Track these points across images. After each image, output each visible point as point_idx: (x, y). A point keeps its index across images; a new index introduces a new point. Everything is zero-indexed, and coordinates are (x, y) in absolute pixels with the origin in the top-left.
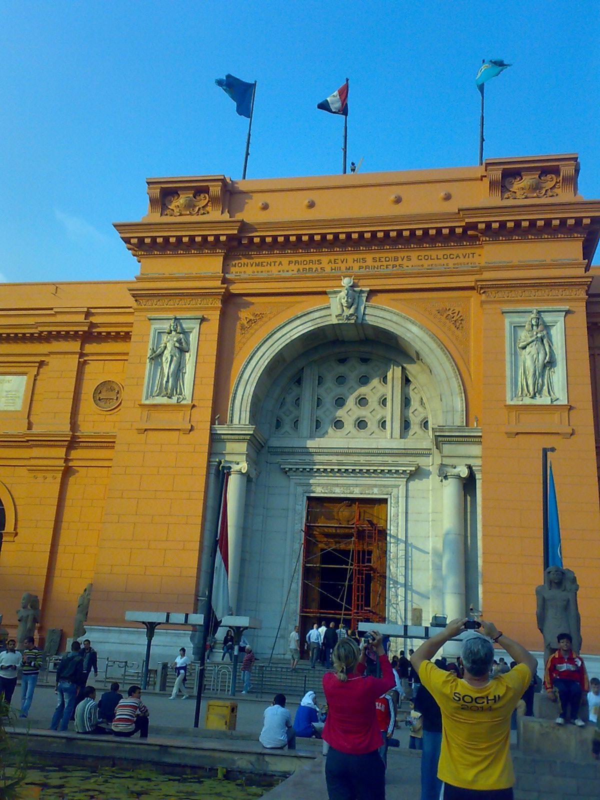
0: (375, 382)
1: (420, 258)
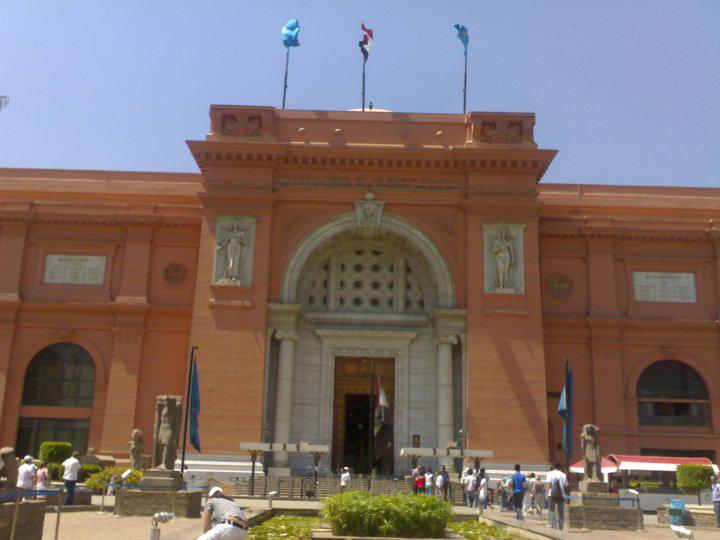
0: (385, 270)
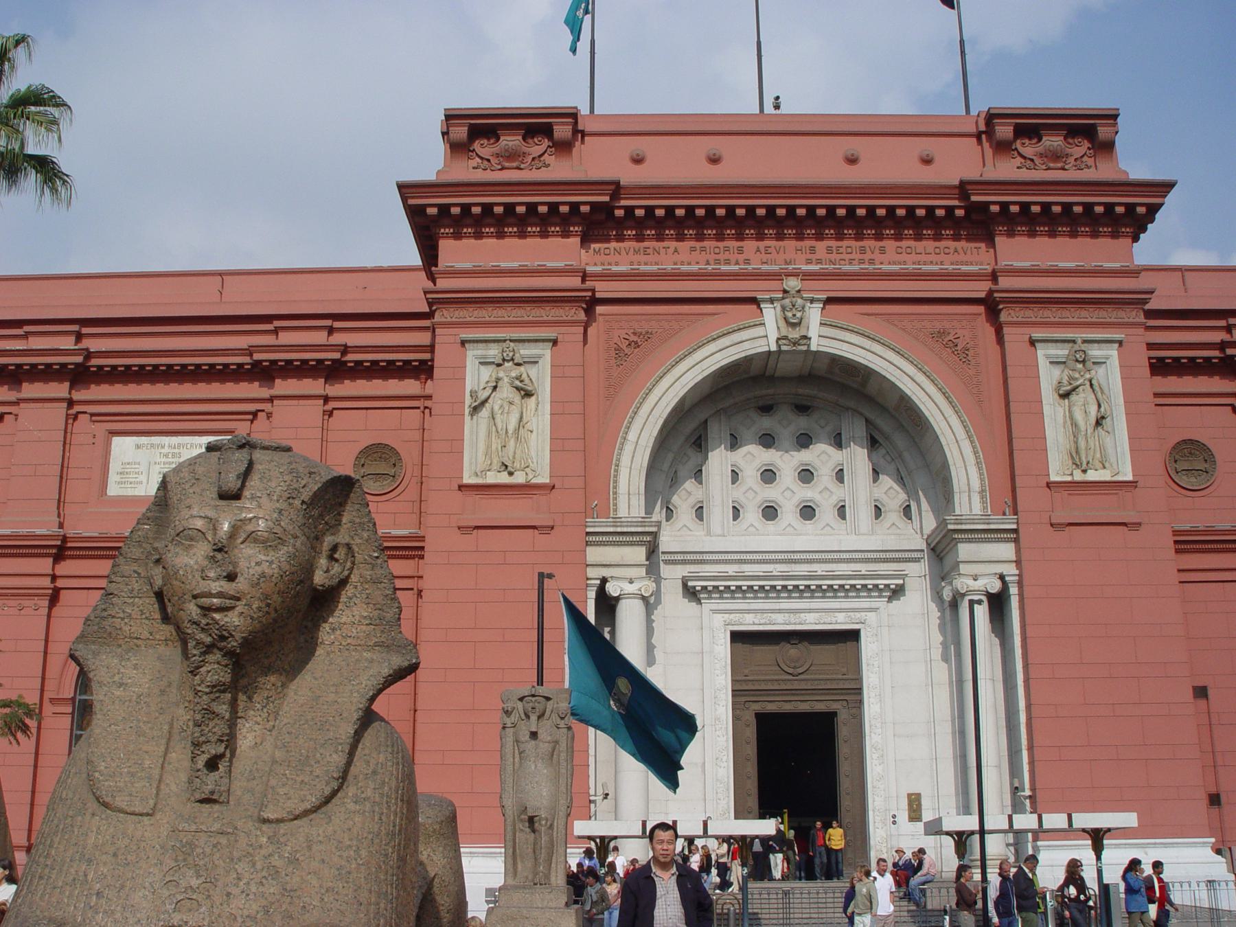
1: (899, 250)
